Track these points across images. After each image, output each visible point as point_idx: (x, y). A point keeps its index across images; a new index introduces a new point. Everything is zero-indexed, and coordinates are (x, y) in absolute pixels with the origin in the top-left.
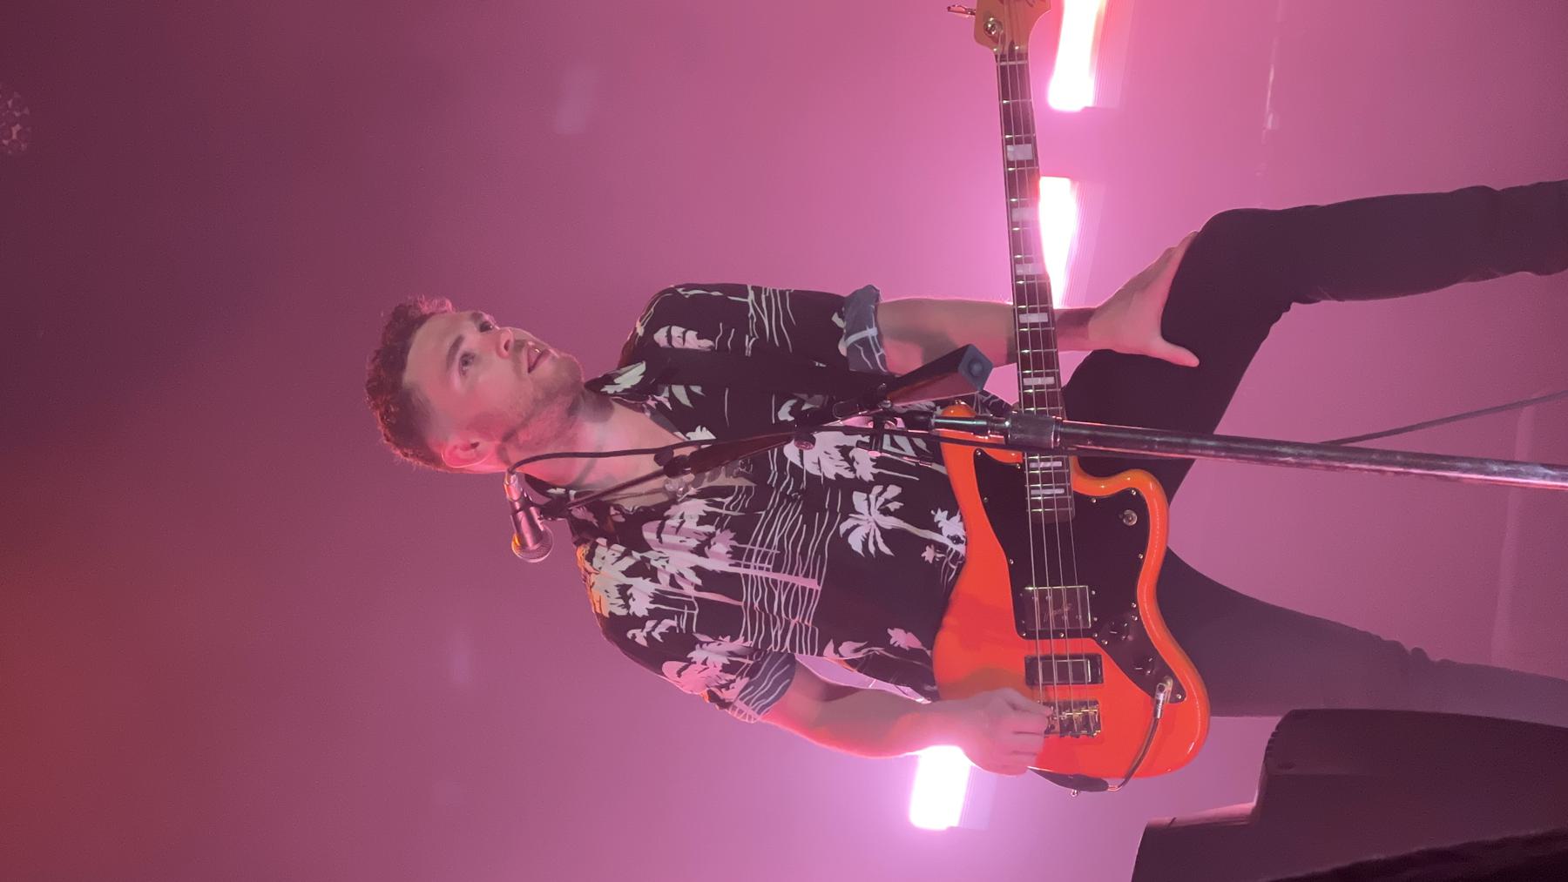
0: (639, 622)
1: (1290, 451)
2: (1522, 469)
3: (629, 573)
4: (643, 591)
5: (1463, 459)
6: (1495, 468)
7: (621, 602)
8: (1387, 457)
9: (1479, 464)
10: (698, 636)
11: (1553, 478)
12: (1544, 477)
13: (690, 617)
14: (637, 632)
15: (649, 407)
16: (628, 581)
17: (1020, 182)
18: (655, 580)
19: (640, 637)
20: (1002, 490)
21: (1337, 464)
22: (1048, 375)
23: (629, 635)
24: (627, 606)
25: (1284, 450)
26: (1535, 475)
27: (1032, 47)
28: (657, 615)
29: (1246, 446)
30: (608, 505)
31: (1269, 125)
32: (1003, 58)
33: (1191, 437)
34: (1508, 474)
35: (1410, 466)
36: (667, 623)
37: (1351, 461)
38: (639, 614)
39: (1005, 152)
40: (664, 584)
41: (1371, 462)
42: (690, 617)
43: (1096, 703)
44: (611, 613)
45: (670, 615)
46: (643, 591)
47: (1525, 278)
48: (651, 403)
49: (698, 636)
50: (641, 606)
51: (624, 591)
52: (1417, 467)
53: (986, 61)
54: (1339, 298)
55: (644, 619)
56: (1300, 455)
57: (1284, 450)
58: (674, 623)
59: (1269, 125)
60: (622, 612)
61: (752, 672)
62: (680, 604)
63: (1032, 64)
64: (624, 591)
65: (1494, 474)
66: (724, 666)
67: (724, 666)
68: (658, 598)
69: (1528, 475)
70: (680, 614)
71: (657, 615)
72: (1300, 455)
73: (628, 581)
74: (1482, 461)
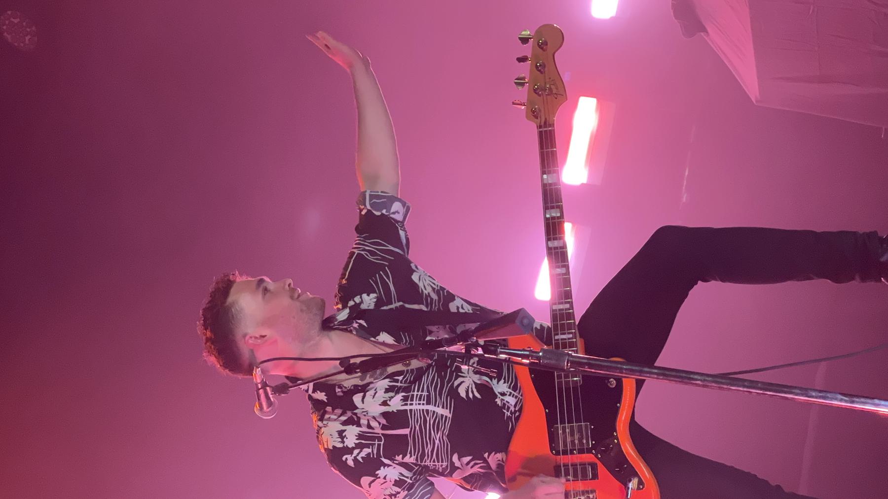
0: (349, 451)
1: (699, 378)
2: (829, 395)
3: (345, 423)
4: (352, 433)
5: (795, 388)
6: (814, 394)
7: (340, 440)
8: (753, 384)
9: (805, 391)
10: (383, 459)
11: (846, 401)
12: (841, 400)
13: (379, 445)
14: (348, 456)
15: (355, 328)
16: (344, 428)
17: (553, 229)
18: (359, 425)
19: (349, 460)
20: (543, 379)
21: (725, 387)
22: (566, 303)
23: (344, 459)
24: (343, 442)
25: (696, 377)
26: (836, 399)
27: (556, 119)
28: (360, 446)
29: (674, 373)
30: (334, 386)
31: (684, 200)
32: (540, 127)
33: (644, 367)
34: (820, 397)
35: (766, 390)
36: (366, 451)
37: (734, 385)
38: (350, 446)
39: (542, 177)
40: (365, 429)
41: (744, 386)
42: (379, 445)
43: (595, 491)
44: (334, 447)
45: (368, 446)
46: (352, 433)
47: (824, 284)
48: (356, 325)
49: (383, 459)
50: (351, 441)
51: (341, 434)
52: (770, 391)
53: (531, 131)
54: (723, 281)
55: (353, 449)
56: (705, 380)
57: (696, 377)
58: (370, 450)
59: (684, 200)
60: (340, 445)
61: (411, 486)
62: (373, 439)
63: (558, 149)
64: (341, 434)
65: (813, 397)
66: (396, 481)
67: (396, 481)
68: (360, 436)
69: (832, 399)
70: (373, 445)
71: (360, 446)
72: (705, 380)
73: (344, 428)
74: (806, 390)
